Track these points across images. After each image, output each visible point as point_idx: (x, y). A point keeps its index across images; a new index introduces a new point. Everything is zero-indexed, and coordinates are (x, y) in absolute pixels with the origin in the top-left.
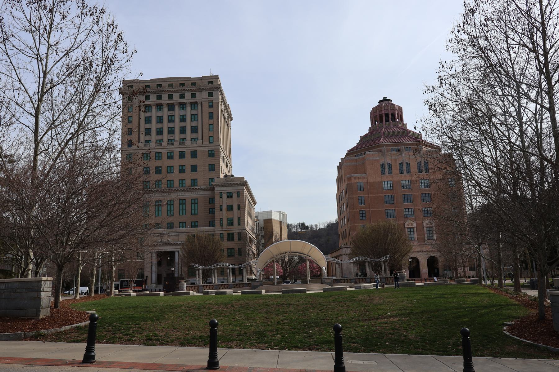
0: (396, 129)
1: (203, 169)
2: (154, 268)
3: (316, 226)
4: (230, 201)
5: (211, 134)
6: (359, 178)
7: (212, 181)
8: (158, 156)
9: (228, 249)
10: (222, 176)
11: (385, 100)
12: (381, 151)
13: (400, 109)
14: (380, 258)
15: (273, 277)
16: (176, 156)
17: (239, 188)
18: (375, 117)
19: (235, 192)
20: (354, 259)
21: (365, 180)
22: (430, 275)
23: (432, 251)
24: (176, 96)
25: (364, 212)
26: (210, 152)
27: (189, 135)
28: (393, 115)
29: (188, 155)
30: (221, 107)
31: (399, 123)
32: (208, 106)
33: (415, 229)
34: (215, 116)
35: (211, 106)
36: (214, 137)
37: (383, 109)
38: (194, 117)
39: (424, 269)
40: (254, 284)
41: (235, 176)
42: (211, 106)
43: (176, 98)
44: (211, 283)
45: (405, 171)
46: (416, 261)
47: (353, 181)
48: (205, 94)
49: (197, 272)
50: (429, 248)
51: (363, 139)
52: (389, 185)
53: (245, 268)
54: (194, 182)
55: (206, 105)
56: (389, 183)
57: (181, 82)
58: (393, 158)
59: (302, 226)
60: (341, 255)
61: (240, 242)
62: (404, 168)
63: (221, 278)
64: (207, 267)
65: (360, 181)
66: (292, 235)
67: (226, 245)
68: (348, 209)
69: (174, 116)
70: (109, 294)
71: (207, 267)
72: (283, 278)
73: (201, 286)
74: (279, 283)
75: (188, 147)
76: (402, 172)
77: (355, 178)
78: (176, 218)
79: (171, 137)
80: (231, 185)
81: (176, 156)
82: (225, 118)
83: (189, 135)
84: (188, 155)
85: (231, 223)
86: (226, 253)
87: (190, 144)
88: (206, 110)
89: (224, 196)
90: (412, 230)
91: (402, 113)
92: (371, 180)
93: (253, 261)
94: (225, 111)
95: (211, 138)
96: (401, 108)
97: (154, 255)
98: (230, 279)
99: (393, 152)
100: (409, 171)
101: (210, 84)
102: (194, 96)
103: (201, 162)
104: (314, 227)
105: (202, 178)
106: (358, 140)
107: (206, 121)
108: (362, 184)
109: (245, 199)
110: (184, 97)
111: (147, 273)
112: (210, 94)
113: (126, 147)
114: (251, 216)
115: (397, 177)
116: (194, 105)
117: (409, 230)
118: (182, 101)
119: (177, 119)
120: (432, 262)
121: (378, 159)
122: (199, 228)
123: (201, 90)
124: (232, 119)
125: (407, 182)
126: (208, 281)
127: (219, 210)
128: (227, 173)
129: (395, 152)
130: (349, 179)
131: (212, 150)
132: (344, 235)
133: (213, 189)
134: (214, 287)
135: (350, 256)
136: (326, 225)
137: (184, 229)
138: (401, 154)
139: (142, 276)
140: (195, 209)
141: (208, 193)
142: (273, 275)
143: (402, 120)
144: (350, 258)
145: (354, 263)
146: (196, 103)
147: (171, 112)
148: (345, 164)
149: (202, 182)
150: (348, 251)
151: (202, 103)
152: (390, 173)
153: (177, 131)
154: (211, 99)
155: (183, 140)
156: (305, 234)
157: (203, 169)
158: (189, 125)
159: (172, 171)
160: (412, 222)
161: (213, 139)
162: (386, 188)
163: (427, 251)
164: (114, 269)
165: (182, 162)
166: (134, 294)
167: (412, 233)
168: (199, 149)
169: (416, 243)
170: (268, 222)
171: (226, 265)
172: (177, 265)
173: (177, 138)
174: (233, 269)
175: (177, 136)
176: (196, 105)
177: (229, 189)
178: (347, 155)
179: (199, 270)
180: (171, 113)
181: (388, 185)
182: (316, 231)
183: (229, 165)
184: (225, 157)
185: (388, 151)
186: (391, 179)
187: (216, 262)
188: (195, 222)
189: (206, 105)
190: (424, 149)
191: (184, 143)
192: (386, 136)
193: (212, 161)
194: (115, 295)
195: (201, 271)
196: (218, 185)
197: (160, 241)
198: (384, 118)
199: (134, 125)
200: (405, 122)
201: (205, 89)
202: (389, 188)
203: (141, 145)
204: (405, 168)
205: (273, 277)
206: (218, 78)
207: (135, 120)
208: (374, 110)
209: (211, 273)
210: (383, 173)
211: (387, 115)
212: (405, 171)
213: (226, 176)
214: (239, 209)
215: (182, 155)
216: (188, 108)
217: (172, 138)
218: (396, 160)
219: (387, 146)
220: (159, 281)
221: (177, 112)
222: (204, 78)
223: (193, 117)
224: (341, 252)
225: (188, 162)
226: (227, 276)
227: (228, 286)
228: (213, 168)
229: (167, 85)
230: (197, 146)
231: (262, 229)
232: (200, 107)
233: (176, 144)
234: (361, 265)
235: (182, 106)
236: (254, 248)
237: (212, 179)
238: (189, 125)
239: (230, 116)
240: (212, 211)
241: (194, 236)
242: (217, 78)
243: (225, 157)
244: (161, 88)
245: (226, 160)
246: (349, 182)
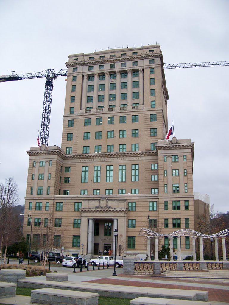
5: (153, 99)
9: (173, 219)
27: (130, 100)
36: (156, 102)
38: (135, 84)
43: (118, 67)
73: (157, 263)
83: (130, 100)
87: (131, 109)
97: (91, 223)
102: (135, 63)
113: (69, 113)
116: (135, 72)
118: (124, 69)
123: (142, 58)
133: (156, 154)
151: (143, 70)
159: (112, 136)
180: (112, 81)
189: (147, 71)
199: (77, 94)
203: (83, 111)
207: (78, 88)
221: (118, 80)
227: (198, 266)
229: (110, 56)
244: (104, 59)
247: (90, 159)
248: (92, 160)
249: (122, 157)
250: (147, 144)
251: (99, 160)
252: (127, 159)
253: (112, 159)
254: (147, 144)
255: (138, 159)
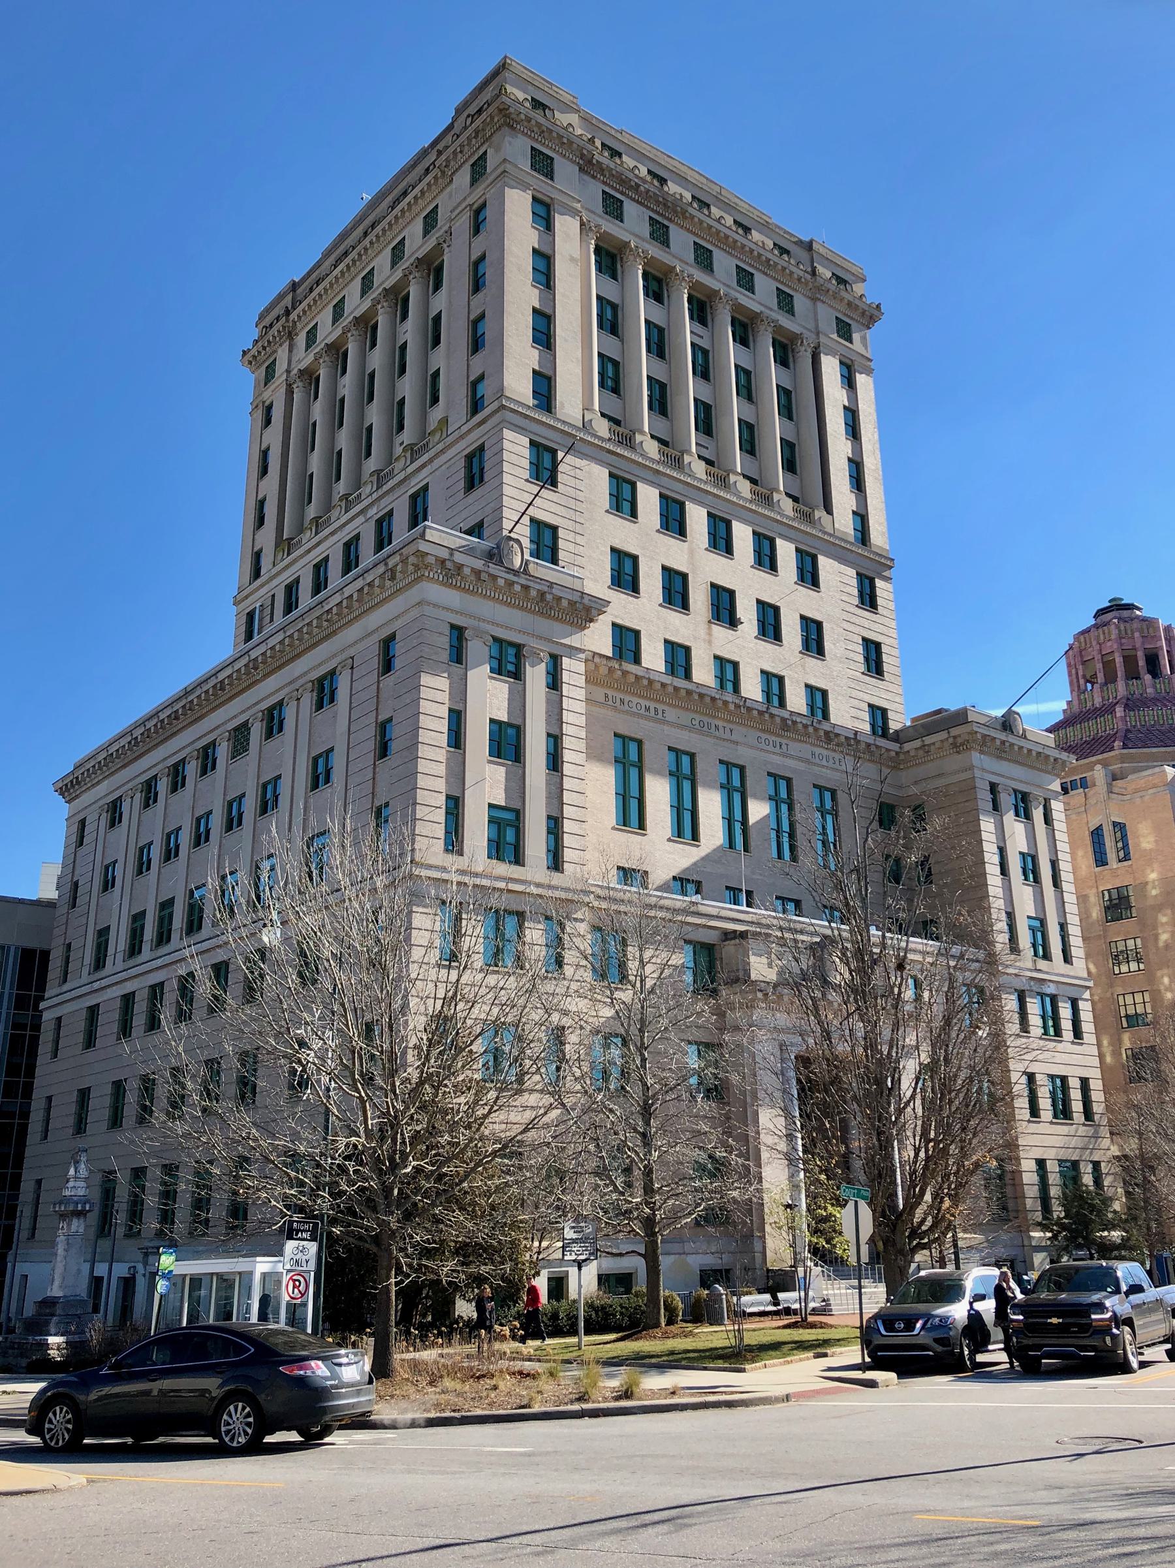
102: (785, 302)
247: (648, 703)
248: (656, 710)
249: (779, 736)
250: (856, 703)
251: (686, 717)
252: (795, 748)
253: (739, 733)
254: (856, 703)
255: (830, 764)
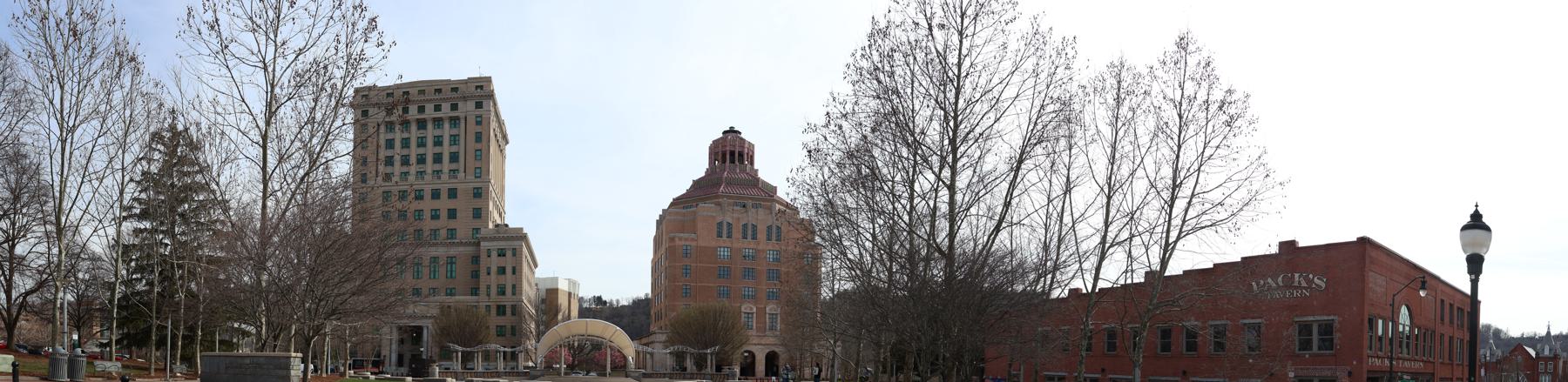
0: (743, 176)
1: (464, 215)
2: (394, 347)
3: (618, 301)
4: (501, 262)
5: (478, 164)
6: (686, 240)
7: (477, 233)
8: (403, 195)
10: (491, 226)
11: (732, 131)
12: (719, 204)
13: (751, 146)
14: (707, 348)
15: (558, 366)
16: (427, 195)
17: (516, 243)
18: (717, 153)
19: (509, 249)
20: (672, 348)
21: (694, 244)
22: (767, 375)
23: (776, 344)
24: (429, 108)
25: (688, 287)
26: (476, 191)
27: (446, 165)
28: (741, 155)
29: (444, 195)
30: (494, 125)
31: (749, 166)
32: (474, 122)
33: (755, 315)
34: (484, 138)
35: (479, 123)
36: (483, 169)
37: (728, 144)
38: (454, 139)
39: (760, 367)
40: (533, 373)
41: (510, 226)
42: (479, 123)
43: (430, 111)
44: (473, 369)
45: (749, 237)
46: (752, 355)
47: (678, 242)
48: (471, 105)
49: (455, 354)
50: (771, 340)
51: (697, 184)
52: (726, 253)
53: (521, 352)
54: (452, 232)
55: (471, 121)
56: (726, 250)
57: (436, 87)
58: (735, 215)
59: (599, 300)
60: (652, 342)
61: (513, 318)
62: (750, 232)
63: (485, 364)
64: (468, 349)
65: (687, 243)
66: (584, 313)
67: (494, 320)
68: (667, 281)
69: (425, 137)
70: (343, 374)
71: (468, 349)
72: (571, 368)
74: (566, 374)
75: (444, 184)
76: (745, 237)
77: (680, 239)
78: (425, 284)
79: (421, 168)
80: (504, 239)
81: (427, 195)
82: (498, 141)
83: (446, 165)
84: (444, 195)
85: (502, 292)
86: (493, 331)
88: (473, 128)
89: (494, 254)
90: (750, 316)
91: (753, 153)
92: (702, 243)
93: (530, 344)
94: (498, 130)
95: (478, 171)
96: (753, 145)
98: (501, 366)
99: (735, 208)
100: (754, 238)
101: (479, 90)
102: (454, 107)
103: (463, 205)
104: (615, 303)
105: (463, 227)
106: (688, 185)
107: (472, 145)
108: (689, 248)
109: (524, 259)
110: (440, 110)
111: (385, 352)
112: (479, 105)
114: (530, 284)
115: (738, 243)
116: (454, 121)
117: (746, 315)
119: (430, 142)
120: (771, 359)
121: (714, 214)
122: (457, 297)
123: (465, 99)
124: (507, 143)
125: (751, 251)
126: (468, 367)
127: (485, 274)
128: (499, 222)
129: (738, 208)
130: (672, 239)
131: (478, 188)
132: (659, 317)
133: (478, 244)
134: (477, 375)
135: (666, 344)
136: (631, 301)
137: (436, 298)
138: (746, 212)
139: (379, 356)
140: (451, 271)
141: (470, 250)
142: (559, 363)
143: (752, 163)
144: (666, 347)
145: (670, 353)
146: (458, 118)
147: (421, 131)
148: (668, 217)
149: (463, 233)
150: (663, 338)
151: (466, 118)
152: (729, 236)
153: (429, 159)
154: (479, 111)
155: (438, 173)
156: (601, 311)
157: (464, 215)
158: (446, 150)
160: (751, 306)
161: (481, 172)
162: (722, 257)
163: (768, 344)
164: (349, 345)
165: (436, 204)
166: (373, 377)
167: (750, 320)
168: (460, 187)
169: (754, 333)
170: (553, 293)
171: (493, 346)
172: (425, 345)
173: (429, 171)
174: (504, 352)
175: (429, 167)
176: (457, 122)
177: (502, 244)
178: (672, 205)
179: (457, 352)
180: (421, 133)
181: (723, 253)
182: (617, 307)
183: (501, 210)
184: (496, 199)
185: (729, 204)
186: (729, 245)
187: (480, 343)
188: (451, 289)
189: (471, 121)
190: (778, 206)
191: (439, 178)
192: (730, 183)
193: (477, 203)
194: (350, 377)
195: (460, 354)
196: (485, 239)
197: (402, 311)
198: (728, 156)
200: (756, 167)
201: (472, 97)
202: (726, 257)
204: (750, 232)
205: (558, 366)
206: (490, 81)
208: (716, 144)
209: (474, 357)
210: (720, 235)
211: (732, 153)
212: (749, 237)
213: (497, 226)
214: (514, 273)
215: (436, 195)
216: (447, 125)
217: (422, 170)
218: (738, 219)
219: (731, 197)
220: (400, 363)
221: (431, 132)
222: (470, 80)
223: (452, 138)
224: (652, 338)
225: (444, 204)
226: (496, 361)
228: (479, 213)
229: (417, 92)
230: (456, 181)
231: (543, 301)
232: (463, 125)
233: (428, 178)
234: (679, 357)
235: (438, 122)
236: (533, 326)
237: (477, 230)
238: (446, 150)
239: (505, 137)
240: (475, 275)
241: (449, 307)
242: (488, 80)
243: (496, 199)
245: (498, 203)
246: (671, 244)
